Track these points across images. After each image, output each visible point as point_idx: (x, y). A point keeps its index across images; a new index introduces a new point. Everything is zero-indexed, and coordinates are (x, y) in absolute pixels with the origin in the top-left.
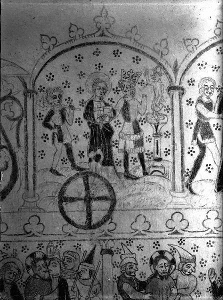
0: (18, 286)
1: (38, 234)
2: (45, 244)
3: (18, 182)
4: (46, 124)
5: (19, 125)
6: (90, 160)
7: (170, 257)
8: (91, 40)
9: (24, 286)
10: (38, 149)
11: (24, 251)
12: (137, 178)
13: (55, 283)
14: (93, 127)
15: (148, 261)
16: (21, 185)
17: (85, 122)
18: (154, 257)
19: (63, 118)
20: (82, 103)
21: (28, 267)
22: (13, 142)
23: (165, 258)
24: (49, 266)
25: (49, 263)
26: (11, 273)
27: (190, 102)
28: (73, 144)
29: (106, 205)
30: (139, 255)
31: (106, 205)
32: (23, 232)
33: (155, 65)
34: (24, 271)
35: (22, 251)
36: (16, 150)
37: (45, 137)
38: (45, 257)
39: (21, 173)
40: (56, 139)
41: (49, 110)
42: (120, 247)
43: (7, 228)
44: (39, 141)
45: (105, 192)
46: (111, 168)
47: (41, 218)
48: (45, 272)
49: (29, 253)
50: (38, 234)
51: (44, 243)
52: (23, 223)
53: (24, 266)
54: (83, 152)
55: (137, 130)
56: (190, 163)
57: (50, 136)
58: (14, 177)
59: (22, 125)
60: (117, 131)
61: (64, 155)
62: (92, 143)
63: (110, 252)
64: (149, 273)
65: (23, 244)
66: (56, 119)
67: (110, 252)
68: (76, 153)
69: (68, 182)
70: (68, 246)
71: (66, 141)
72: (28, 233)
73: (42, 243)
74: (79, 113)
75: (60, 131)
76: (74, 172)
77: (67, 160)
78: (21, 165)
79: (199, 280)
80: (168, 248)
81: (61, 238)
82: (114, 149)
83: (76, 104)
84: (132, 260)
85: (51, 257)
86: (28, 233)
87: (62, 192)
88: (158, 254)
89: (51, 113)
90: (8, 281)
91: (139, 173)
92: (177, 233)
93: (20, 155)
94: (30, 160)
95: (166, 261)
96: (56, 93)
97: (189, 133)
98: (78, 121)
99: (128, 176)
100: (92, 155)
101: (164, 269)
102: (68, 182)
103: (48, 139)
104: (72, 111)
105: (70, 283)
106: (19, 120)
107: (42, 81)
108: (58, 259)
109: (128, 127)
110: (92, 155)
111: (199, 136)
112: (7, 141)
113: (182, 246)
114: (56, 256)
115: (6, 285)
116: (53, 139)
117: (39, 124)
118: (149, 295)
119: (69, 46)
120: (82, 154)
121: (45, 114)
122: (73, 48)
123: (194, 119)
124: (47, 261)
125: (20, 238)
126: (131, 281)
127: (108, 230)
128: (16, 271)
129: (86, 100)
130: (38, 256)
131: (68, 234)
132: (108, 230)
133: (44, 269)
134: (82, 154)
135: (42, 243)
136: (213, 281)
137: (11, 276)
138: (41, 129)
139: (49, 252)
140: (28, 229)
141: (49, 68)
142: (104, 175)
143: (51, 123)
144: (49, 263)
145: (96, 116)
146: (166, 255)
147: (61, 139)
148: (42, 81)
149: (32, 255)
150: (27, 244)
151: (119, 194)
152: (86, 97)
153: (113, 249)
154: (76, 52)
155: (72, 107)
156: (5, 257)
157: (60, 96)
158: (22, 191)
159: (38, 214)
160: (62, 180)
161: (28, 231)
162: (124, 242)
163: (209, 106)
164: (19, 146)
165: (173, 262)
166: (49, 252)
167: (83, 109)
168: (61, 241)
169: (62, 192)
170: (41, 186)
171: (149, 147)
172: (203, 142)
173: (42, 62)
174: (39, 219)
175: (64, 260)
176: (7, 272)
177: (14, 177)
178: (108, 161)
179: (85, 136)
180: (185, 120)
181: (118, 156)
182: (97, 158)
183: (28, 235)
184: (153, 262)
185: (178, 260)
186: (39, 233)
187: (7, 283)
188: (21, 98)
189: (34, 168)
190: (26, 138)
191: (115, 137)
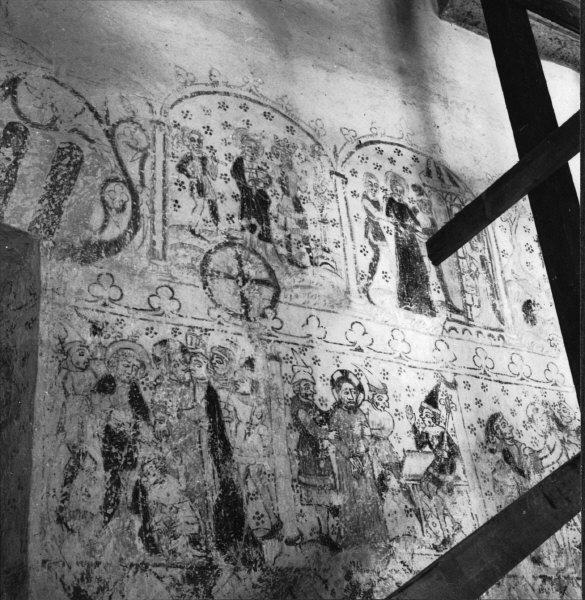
0: (141, 387)
2: (184, 330)
3: (140, 233)
4: (181, 169)
6: (243, 229)
7: (356, 382)
9: (151, 388)
10: (169, 196)
12: (305, 267)
13: (201, 393)
14: (244, 188)
15: (329, 382)
16: (144, 238)
17: (233, 183)
18: (335, 378)
21: (157, 360)
23: (350, 381)
26: (128, 366)
27: (354, 194)
28: (218, 201)
29: (268, 292)
30: (318, 371)
31: (268, 292)
32: (147, 307)
33: (313, 143)
34: (150, 363)
36: (139, 189)
38: (184, 350)
39: (145, 223)
40: (195, 191)
42: (291, 354)
43: (122, 295)
45: (264, 275)
46: (269, 246)
48: (185, 371)
49: (157, 339)
51: (180, 327)
52: (147, 294)
53: (151, 357)
54: (233, 216)
55: (299, 209)
56: (365, 267)
57: (187, 185)
58: (135, 223)
59: (148, 164)
60: (274, 203)
61: (207, 213)
62: (243, 208)
63: (275, 358)
64: (331, 401)
67: (275, 358)
70: (215, 340)
71: (209, 197)
72: (154, 309)
74: (226, 168)
78: (144, 210)
79: (396, 419)
80: (351, 368)
81: (207, 325)
82: (272, 222)
84: (309, 378)
87: (206, 260)
88: (339, 375)
89: (188, 159)
90: (124, 378)
91: (306, 260)
92: (360, 350)
95: (351, 386)
96: (196, 137)
97: (359, 229)
99: (292, 262)
100: (244, 223)
101: (350, 396)
104: (215, 164)
105: (222, 394)
107: (175, 115)
109: (287, 202)
110: (244, 223)
111: (370, 235)
112: (125, 173)
113: (368, 368)
114: (201, 350)
115: (119, 384)
116: (192, 189)
117: (172, 166)
118: (334, 432)
119: (210, 89)
120: (231, 218)
122: (215, 93)
123: (363, 216)
126: (310, 406)
127: (272, 328)
130: (174, 346)
132: (272, 328)
133: (182, 367)
134: (231, 218)
136: (413, 422)
137: (129, 370)
138: (173, 175)
139: (189, 342)
140: (155, 302)
141: (186, 105)
142: (260, 250)
145: (247, 175)
146: (351, 376)
147: (201, 191)
148: (175, 115)
149: (164, 342)
150: (155, 325)
151: (285, 281)
152: (236, 152)
153: (281, 356)
158: (145, 249)
159: (172, 285)
161: (156, 306)
162: (295, 348)
163: (376, 204)
164: (143, 184)
165: (360, 388)
166: (189, 342)
167: (230, 165)
168: (206, 330)
169: (206, 260)
170: (174, 247)
171: (313, 231)
172: (375, 243)
174: (173, 292)
175: (212, 359)
177: (135, 223)
178: (266, 237)
179: (235, 197)
180: (353, 213)
181: (277, 234)
182: (252, 228)
184: (335, 384)
185: (366, 388)
187: (124, 382)
189: (164, 222)
191: (273, 209)
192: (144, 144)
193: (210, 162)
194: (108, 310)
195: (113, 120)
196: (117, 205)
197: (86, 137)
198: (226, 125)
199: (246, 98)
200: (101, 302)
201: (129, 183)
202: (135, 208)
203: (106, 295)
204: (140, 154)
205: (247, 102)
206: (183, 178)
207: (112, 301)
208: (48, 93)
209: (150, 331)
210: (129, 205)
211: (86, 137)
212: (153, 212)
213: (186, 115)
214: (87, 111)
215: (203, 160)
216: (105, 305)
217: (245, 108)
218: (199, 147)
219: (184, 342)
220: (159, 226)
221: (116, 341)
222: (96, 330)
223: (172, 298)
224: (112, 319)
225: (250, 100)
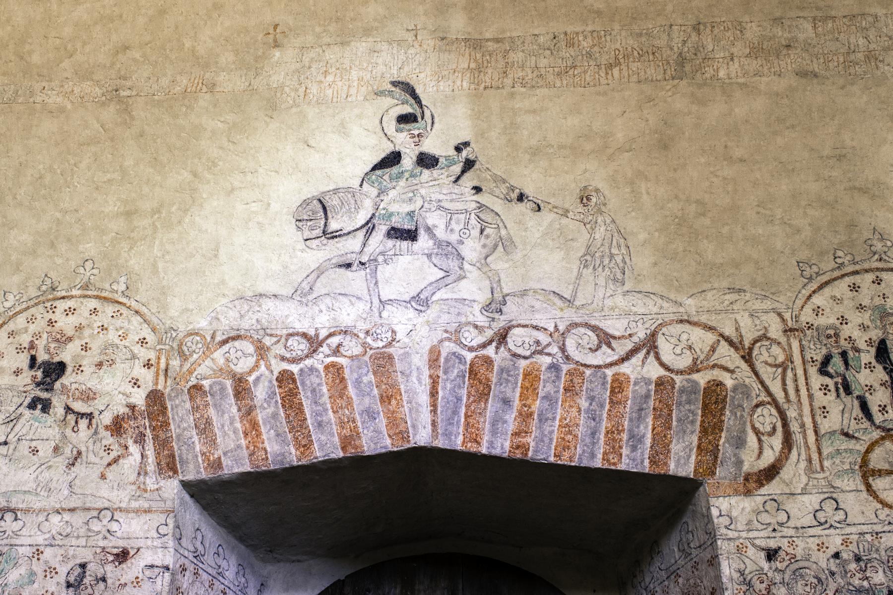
1: (838, 525)
3: (794, 452)
4: (823, 372)
5: (784, 374)
8: (866, 266)
10: (816, 404)
11: (822, 550)
16: (799, 455)
19: (846, 363)
20: (870, 342)
22: (780, 396)
24: (865, 571)
25: (866, 567)
26: (807, 585)
28: (867, 395)
34: (827, 578)
35: (819, 550)
36: (786, 406)
37: (826, 387)
39: (798, 438)
40: (841, 390)
41: (824, 351)
44: (818, 395)
47: (839, 501)
48: (862, 579)
50: (838, 525)
51: (852, 537)
53: (827, 572)
54: (885, 406)
57: (832, 387)
59: (790, 374)
61: (857, 411)
65: (817, 541)
66: (837, 364)
68: (874, 410)
69: (869, 450)
71: (857, 393)
73: (848, 537)
74: (869, 356)
75: (844, 379)
76: (876, 434)
77: (862, 418)
78: (794, 427)
81: (878, 528)
83: (862, 345)
85: (867, 557)
86: (821, 524)
87: (865, 463)
93: (792, 414)
94: (808, 421)
96: (832, 332)
98: (869, 366)
102: (869, 450)
103: (829, 391)
104: (857, 354)
106: (784, 367)
108: (878, 560)
116: (837, 390)
117: (813, 371)
119: (837, 274)
120: (883, 409)
121: (819, 358)
122: (843, 276)
124: (862, 564)
125: (811, 531)
128: (815, 581)
129: (874, 338)
131: (887, 522)
134: (883, 409)
135: (848, 537)
138: (817, 380)
139: (861, 550)
143: (830, 369)
144: (866, 567)
147: (848, 390)
148: (807, 316)
149: (837, 555)
152: (876, 334)
154: (848, 280)
155: (858, 350)
156: (793, 561)
157: (837, 335)
158: (803, 465)
159: (835, 496)
160: (862, 447)
161: (823, 520)
164: (788, 401)
166: (861, 550)
167: (873, 351)
168: (877, 533)
169: (865, 463)
170: (831, 456)
173: (806, 292)
174: (837, 502)
176: (799, 583)
177: (788, 442)
179: (883, 384)
183: (823, 527)
186: (839, 522)
188: (783, 340)
189: (816, 432)
190: (797, 390)
192: (781, 358)
193: (851, 354)
194: (778, 534)
195: (747, 344)
196: (768, 428)
197: (726, 369)
198: (861, 307)
199: (878, 269)
200: (771, 529)
201: (775, 402)
202: (785, 425)
203: (773, 521)
204: (780, 370)
205: (878, 273)
206: (827, 380)
207: (781, 524)
208: (684, 337)
209: (821, 546)
210: (779, 425)
211: (726, 369)
212: (803, 426)
213: (817, 311)
214: (723, 342)
215: (844, 354)
216: (774, 530)
217: (878, 281)
218: (836, 342)
219: (856, 551)
220: (811, 438)
221: (792, 563)
222: (771, 555)
223: (837, 509)
224: (784, 543)
225: (883, 270)
